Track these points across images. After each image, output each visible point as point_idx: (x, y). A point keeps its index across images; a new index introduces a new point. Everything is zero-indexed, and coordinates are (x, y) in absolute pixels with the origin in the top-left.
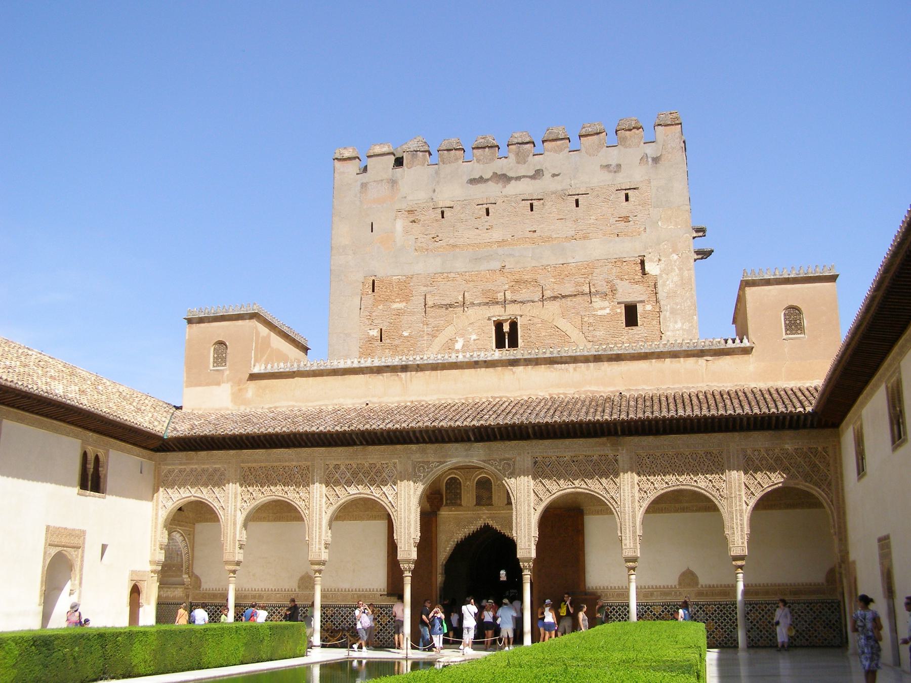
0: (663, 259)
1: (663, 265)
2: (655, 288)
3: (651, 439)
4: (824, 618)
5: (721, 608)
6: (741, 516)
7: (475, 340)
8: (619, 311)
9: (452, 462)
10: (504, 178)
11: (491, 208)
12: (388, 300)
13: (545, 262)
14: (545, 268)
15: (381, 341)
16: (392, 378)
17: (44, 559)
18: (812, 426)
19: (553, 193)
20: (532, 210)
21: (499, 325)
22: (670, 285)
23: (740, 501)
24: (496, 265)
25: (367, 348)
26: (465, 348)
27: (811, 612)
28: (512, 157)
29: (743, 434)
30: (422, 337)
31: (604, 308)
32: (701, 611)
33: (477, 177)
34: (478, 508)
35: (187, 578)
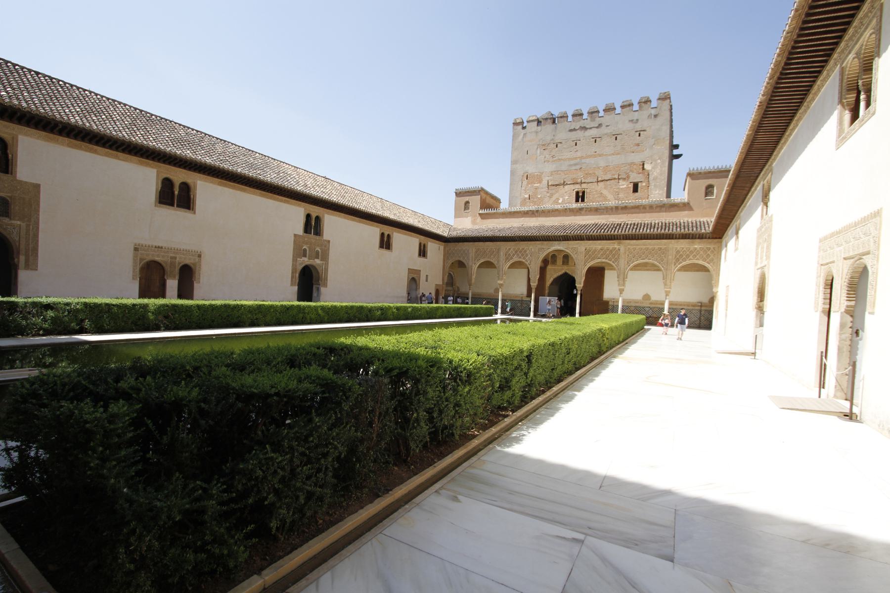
0: (653, 162)
2: (648, 175)
3: (634, 241)
11: (578, 142)
14: (599, 168)
17: (408, 280)
18: (709, 238)
19: (606, 134)
20: (595, 142)
21: (577, 193)
22: (655, 174)
24: (578, 167)
28: (589, 119)
29: (676, 240)
31: (624, 185)
33: (573, 128)
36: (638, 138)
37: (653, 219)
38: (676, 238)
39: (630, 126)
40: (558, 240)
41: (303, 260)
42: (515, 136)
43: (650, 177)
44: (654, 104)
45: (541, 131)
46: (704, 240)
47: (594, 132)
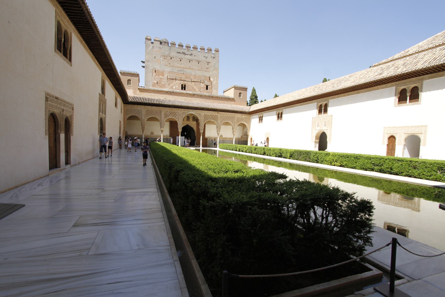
3: (223, 113)
10: (184, 53)
11: (182, 60)
13: (192, 74)
14: (192, 75)
16: (170, 94)
19: (194, 60)
20: (190, 62)
21: (182, 85)
24: (182, 72)
25: (154, 85)
26: (176, 89)
29: (237, 114)
33: (179, 52)
37: (143, 96)
38: (237, 113)
39: (204, 59)
40: (192, 109)
42: (147, 46)
44: (213, 52)
45: (162, 48)
46: (246, 114)
47: (189, 57)
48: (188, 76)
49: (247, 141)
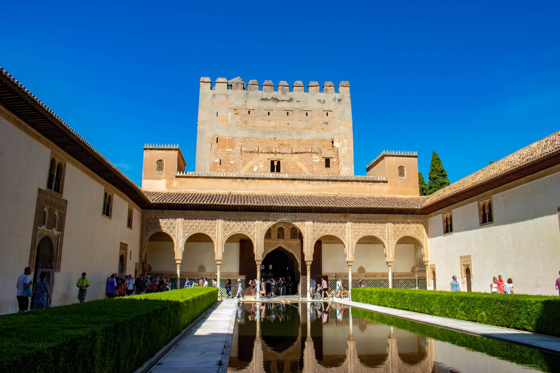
1: (341, 144)
3: (359, 215)
4: (410, 285)
5: (373, 281)
6: (392, 246)
7: (262, 168)
8: (323, 161)
9: (279, 220)
11: (270, 111)
12: (224, 147)
13: (293, 138)
15: (220, 164)
16: (241, 182)
18: (418, 214)
19: (297, 109)
20: (288, 115)
21: (272, 162)
22: (343, 152)
23: (392, 241)
24: (272, 137)
25: (214, 167)
27: (406, 283)
30: (239, 164)
31: (317, 159)
32: (366, 283)
34: (279, 239)
35: (145, 266)
36: (327, 117)
38: (393, 213)
39: (317, 105)
40: (285, 212)
41: (43, 230)
43: (339, 154)
46: (414, 215)
48: (285, 143)
49: (426, 280)
